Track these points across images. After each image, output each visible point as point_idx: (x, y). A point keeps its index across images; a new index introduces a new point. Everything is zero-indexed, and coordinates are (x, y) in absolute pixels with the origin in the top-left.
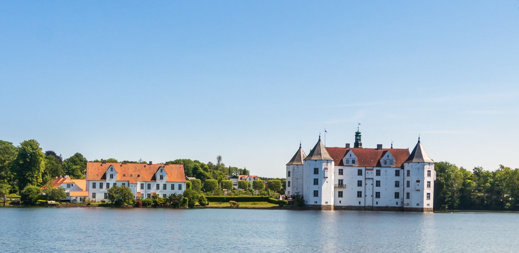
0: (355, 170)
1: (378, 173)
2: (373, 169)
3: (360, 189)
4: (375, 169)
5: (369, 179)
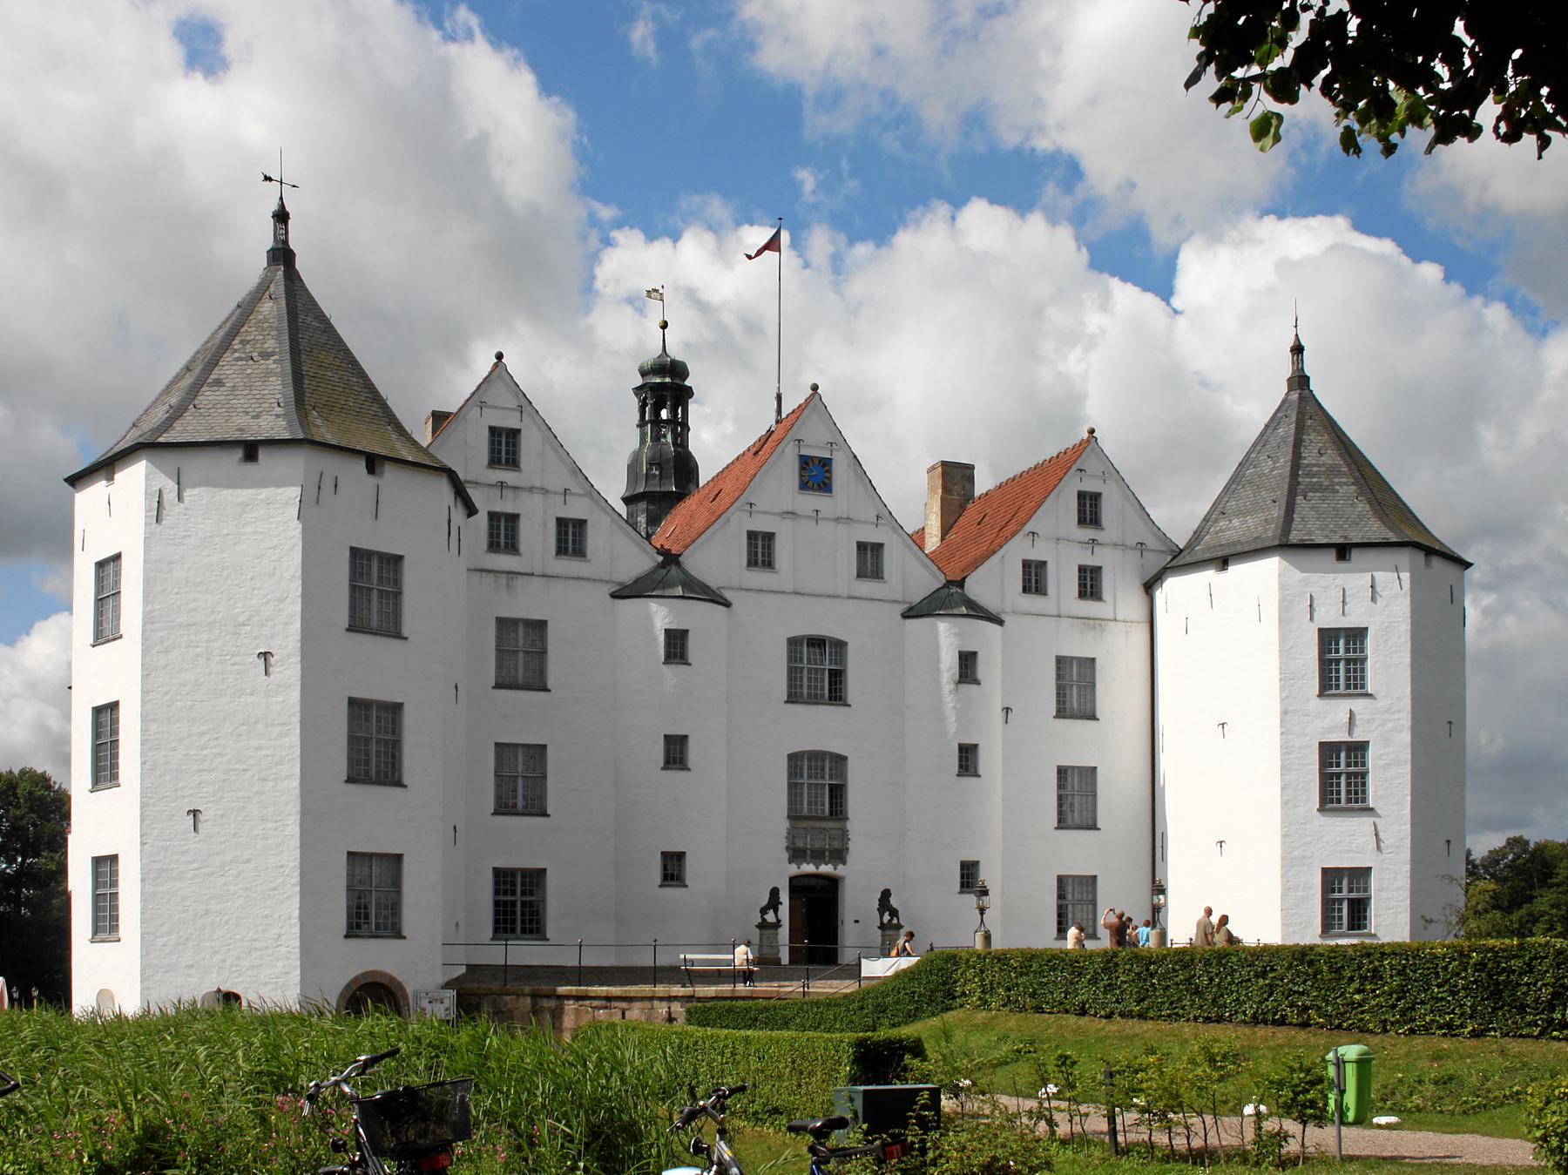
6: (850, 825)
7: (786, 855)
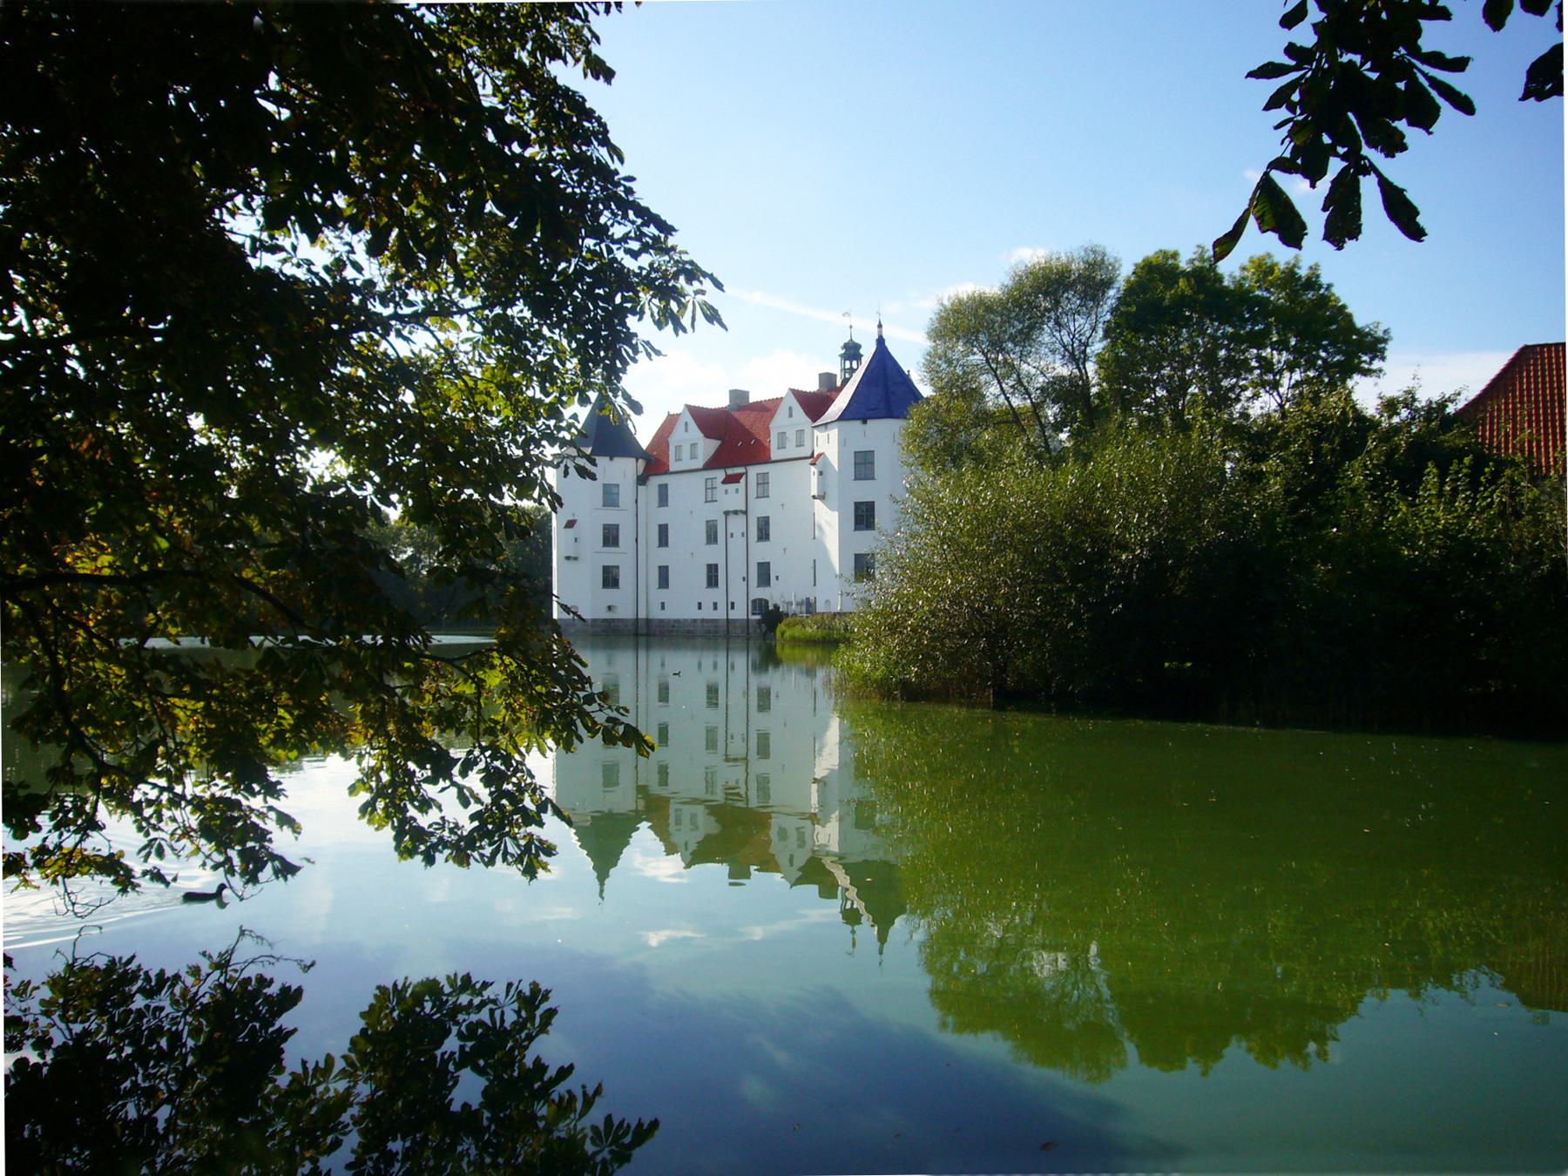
2: (746, 473)
3: (714, 554)
4: (753, 471)
5: (736, 512)
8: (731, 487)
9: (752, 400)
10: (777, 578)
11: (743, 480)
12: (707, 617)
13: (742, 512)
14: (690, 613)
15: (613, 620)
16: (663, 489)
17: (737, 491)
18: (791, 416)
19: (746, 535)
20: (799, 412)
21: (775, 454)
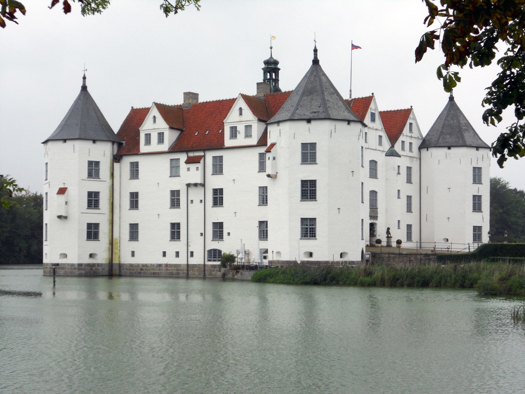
0: (165, 162)
1: (218, 169)
2: (204, 156)
4: (210, 156)
5: (196, 185)
6: (379, 210)
7: (369, 218)
8: (193, 167)
9: (202, 99)
10: (229, 234)
11: (202, 161)
12: (169, 263)
13: (201, 184)
14: (155, 259)
15: (93, 265)
16: (135, 167)
17: (197, 169)
18: (241, 114)
19: (203, 201)
20: (248, 114)
21: (228, 142)
